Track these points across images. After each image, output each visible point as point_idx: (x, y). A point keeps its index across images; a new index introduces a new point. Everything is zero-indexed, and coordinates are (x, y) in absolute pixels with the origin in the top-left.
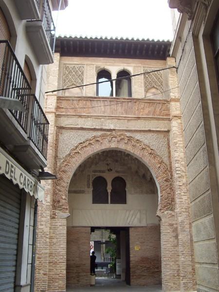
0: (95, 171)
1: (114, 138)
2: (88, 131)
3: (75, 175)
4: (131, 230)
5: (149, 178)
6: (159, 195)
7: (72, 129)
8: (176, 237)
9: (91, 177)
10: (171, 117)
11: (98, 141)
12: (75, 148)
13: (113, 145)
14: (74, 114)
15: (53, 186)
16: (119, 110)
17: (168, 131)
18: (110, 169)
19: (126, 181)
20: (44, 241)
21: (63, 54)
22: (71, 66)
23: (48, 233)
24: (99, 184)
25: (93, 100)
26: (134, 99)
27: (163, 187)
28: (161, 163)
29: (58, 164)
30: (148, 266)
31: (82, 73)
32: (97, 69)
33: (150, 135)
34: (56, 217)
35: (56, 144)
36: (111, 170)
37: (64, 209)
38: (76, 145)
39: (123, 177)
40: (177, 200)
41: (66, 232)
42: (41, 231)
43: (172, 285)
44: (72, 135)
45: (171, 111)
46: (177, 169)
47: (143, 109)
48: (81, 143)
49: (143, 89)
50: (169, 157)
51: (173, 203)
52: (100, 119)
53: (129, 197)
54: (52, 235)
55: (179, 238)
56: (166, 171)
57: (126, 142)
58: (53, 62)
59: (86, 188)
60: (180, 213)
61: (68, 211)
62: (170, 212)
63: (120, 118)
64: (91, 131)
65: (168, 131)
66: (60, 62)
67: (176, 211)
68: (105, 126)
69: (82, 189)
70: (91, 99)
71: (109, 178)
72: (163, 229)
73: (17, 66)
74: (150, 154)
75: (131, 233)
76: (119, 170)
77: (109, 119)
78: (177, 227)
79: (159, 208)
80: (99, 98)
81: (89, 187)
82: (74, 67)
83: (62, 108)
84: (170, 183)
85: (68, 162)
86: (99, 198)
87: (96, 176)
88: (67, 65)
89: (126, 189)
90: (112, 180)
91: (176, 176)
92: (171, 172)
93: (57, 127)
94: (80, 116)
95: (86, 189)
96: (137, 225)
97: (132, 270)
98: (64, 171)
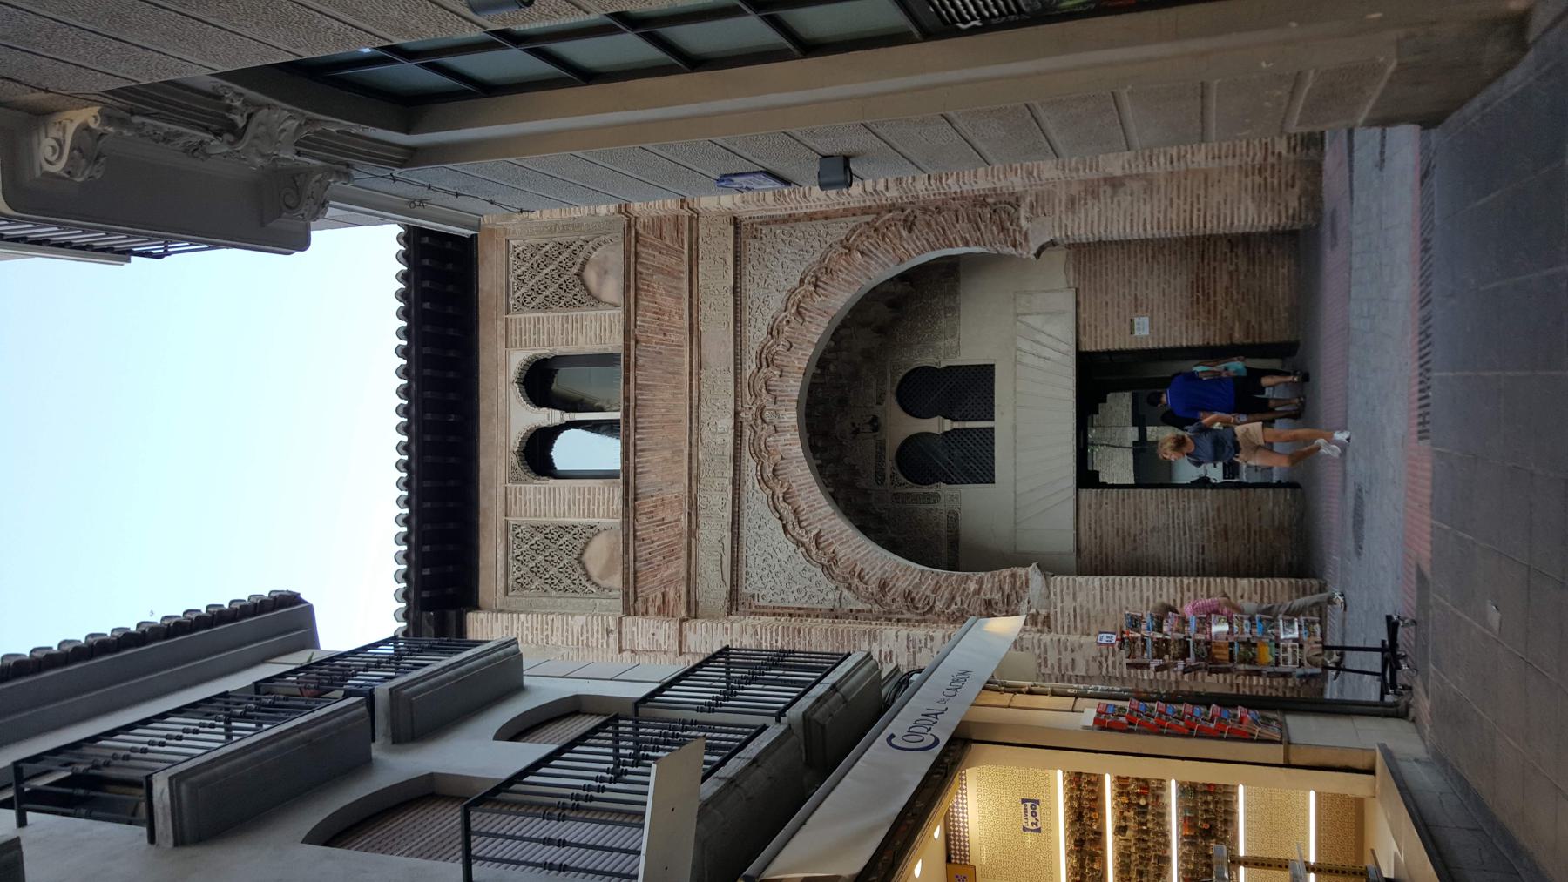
0: (880, 475)
1: (767, 415)
2: (744, 507)
3: (893, 547)
4: (1089, 346)
5: (900, 286)
6: (961, 250)
7: (735, 562)
8: (1115, 183)
9: (899, 490)
10: (685, 213)
11: (774, 470)
13: (790, 417)
14: (684, 554)
16: (664, 402)
17: (736, 222)
18: (871, 422)
21: (471, 602)
22: (512, 569)
26: (627, 347)
29: (860, 606)
30: (1225, 278)
32: (524, 477)
33: (748, 288)
37: (1013, 587)
38: (793, 547)
41: (1097, 579)
43: (1297, 189)
47: (659, 313)
48: (784, 527)
49: (589, 313)
50: (826, 218)
51: (990, 200)
53: (970, 355)
55: (1118, 173)
57: (777, 372)
58: (514, 642)
59: (940, 506)
60: (1031, 173)
61: (1021, 571)
62: (1023, 212)
63: (695, 394)
64: (744, 496)
65: (736, 222)
66: (501, 611)
67: (1019, 189)
68: (723, 445)
70: (631, 496)
72: (1082, 235)
73: (543, 770)
74: (816, 286)
75: (1102, 347)
77: (699, 435)
78: (1080, 181)
79: (1011, 250)
80: (625, 468)
81: (936, 497)
84: (918, 213)
86: (975, 460)
87: (897, 471)
89: (943, 365)
90: (904, 416)
91: (893, 193)
92: (878, 211)
93: (730, 613)
94: (692, 533)
97: (1238, 337)
98: (883, 586)
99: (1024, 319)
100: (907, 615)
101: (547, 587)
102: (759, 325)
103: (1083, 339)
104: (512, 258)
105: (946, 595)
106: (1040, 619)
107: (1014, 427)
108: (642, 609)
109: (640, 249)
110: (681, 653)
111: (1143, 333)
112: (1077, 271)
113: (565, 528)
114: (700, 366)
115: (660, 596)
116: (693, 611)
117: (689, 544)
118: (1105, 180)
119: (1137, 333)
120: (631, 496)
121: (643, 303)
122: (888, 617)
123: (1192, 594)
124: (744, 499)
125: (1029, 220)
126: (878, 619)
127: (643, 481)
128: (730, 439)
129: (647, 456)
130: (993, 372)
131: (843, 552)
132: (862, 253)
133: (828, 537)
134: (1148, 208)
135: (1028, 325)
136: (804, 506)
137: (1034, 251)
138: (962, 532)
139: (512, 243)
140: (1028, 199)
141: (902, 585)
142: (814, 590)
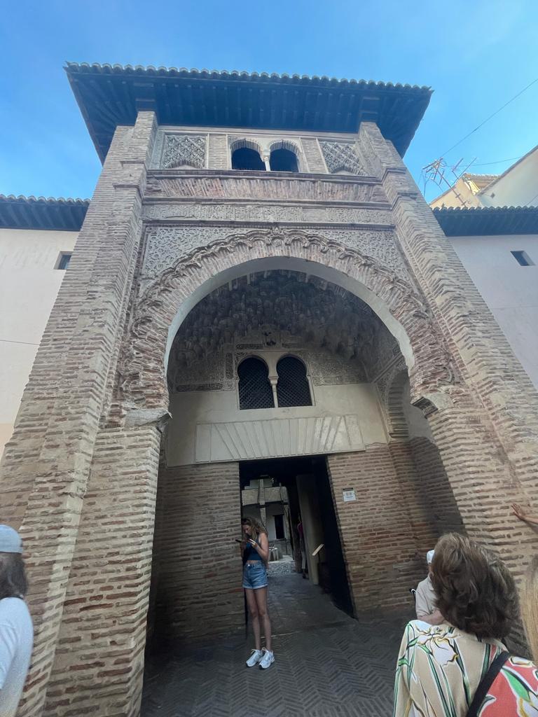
2: (218, 229)
6: (407, 350)
8: (501, 455)
9: (234, 357)
11: (241, 244)
12: (187, 257)
13: (277, 252)
15: (123, 339)
19: (306, 363)
20: (51, 510)
23: (73, 475)
25: (227, 179)
26: (310, 176)
27: (414, 329)
28: (392, 282)
29: (142, 290)
31: (203, 146)
32: (232, 141)
34: (123, 421)
35: (140, 253)
38: (188, 252)
39: (298, 355)
40: (464, 355)
42: (47, 468)
45: (388, 195)
46: (441, 283)
48: (203, 248)
52: (245, 205)
54: (95, 483)
56: (409, 296)
57: (306, 245)
59: (225, 379)
63: (287, 204)
67: (468, 382)
70: (221, 176)
74: (365, 265)
77: (262, 206)
78: (493, 427)
82: (186, 139)
83: (160, 191)
88: (172, 136)
89: (309, 378)
91: (439, 301)
93: (144, 222)
94: (198, 201)
96: (344, 450)
98: (156, 304)
100: (131, 320)
101: (169, 149)
102: (335, 236)
103: (335, 458)
104: (346, 144)
105: (145, 346)
106: (116, 419)
107: (276, 419)
108: (151, 181)
109: (366, 186)
110: (116, 186)
111: (345, 498)
112: (376, 451)
113: (203, 156)
115: (159, 189)
116: (147, 203)
117: (191, 200)
118: (501, 446)
119: (344, 493)
120: (221, 176)
121: (336, 186)
122: (131, 308)
123: (123, 574)
124: (221, 228)
125: (447, 392)
126: (131, 301)
127: (232, 182)
128: (261, 220)
129: (246, 183)
130: (308, 405)
131: (184, 281)
132: (392, 289)
133: (194, 271)
134: (494, 487)
135: (339, 423)
137: (425, 396)
139: (354, 146)
140: (463, 390)
141: (157, 316)
142: (156, 264)
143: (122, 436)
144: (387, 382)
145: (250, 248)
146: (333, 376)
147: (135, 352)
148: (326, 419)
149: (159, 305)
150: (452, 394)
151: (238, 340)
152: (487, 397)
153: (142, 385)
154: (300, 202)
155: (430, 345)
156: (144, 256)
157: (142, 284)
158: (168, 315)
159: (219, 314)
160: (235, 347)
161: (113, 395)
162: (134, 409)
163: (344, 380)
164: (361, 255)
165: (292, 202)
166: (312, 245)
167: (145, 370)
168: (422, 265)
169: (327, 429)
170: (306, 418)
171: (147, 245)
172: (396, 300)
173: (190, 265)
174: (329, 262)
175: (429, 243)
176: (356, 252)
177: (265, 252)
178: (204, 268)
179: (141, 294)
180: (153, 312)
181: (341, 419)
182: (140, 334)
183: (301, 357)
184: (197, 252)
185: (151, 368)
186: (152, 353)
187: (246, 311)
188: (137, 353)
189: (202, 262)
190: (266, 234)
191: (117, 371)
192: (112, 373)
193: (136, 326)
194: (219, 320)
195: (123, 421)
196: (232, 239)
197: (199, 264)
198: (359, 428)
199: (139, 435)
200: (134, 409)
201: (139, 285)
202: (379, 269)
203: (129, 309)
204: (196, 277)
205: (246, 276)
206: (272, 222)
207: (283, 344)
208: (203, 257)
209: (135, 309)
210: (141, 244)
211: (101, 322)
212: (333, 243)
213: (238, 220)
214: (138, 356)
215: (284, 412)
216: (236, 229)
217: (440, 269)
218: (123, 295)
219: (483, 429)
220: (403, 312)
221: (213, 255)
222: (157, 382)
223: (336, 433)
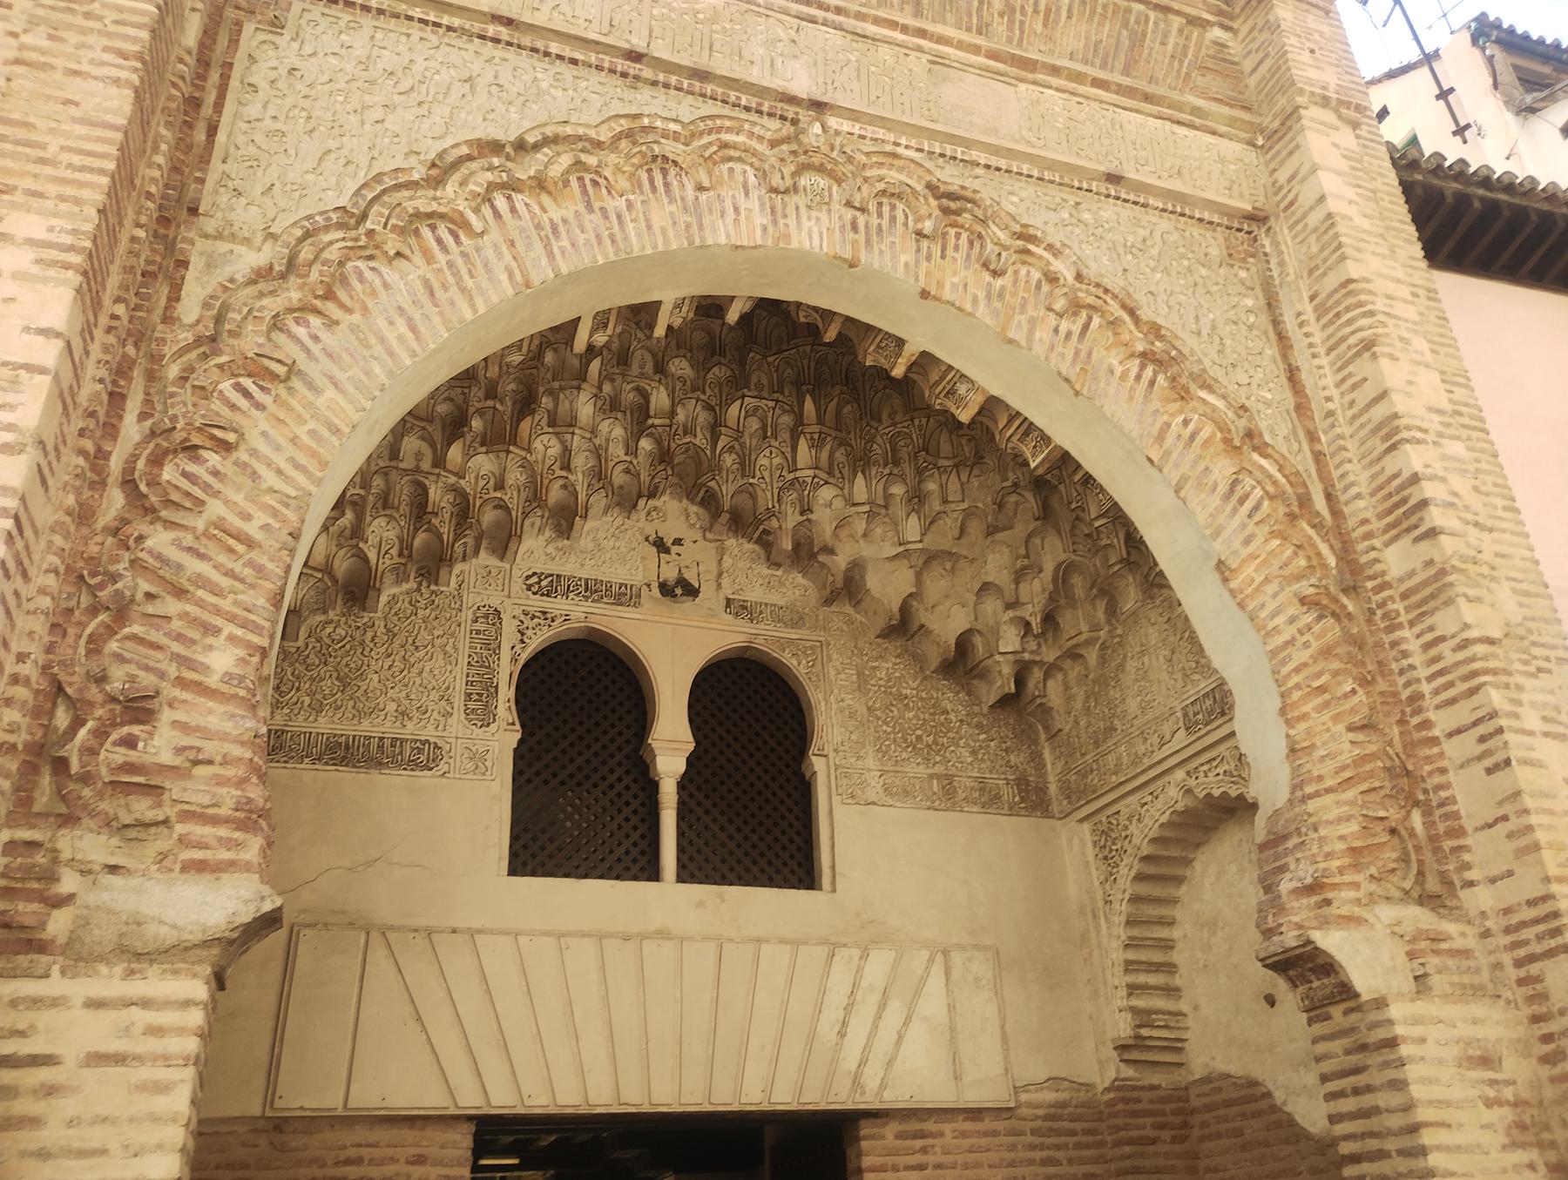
13: (815, 231)
15: (84, 515)
18: (682, 582)
24: (576, 701)
34: (59, 924)
36: (692, 591)
39: (787, 658)
44: (387, 60)
45: (1252, 81)
48: (496, 147)
59: (457, 725)
63: (871, 29)
69: (410, 730)
71: (672, 655)
76: (755, 594)
85: (329, 295)
89: (818, 764)
95: (457, 730)
98: (259, 370)
99: (938, 968)
105: (194, 565)
114: (937, 61)
128: (756, 75)
136: (555, 213)
138: (378, 778)
141: (258, 430)
143: (56, 1002)
144: (1133, 828)
145: (700, 188)
146: (917, 769)
147: (144, 586)
148: (873, 953)
149: (274, 377)
150: (1414, 940)
151: (537, 550)
152: (1534, 969)
153: (167, 758)
154: (922, 33)
155: (1351, 729)
156: (212, 130)
157: (197, 263)
158: (312, 433)
159: (477, 424)
160: (518, 586)
161: (17, 789)
162: (113, 869)
163: (961, 795)
164: (1132, 312)
165: (893, 25)
166: (952, 231)
167: (180, 682)
168: (1352, 404)
169: (873, 1000)
170: (796, 943)
171: (236, 74)
172: (1243, 526)
173: (430, 215)
174: (1009, 318)
175: (1391, 322)
176: (1115, 297)
177: (760, 219)
178: (495, 234)
179: (190, 308)
180: (243, 403)
181: (931, 960)
182: (168, 503)
183: (797, 666)
184: (470, 158)
185: (213, 681)
186: (226, 604)
187: (594, 432)
188: (150, 596)
189: (486, 211)
190: (774, 144)
191: (46, 668)
192: (27, 682)
193: (157, 461)
194: (468, 456)
195: (59, 924)
196: (629, 134)
197: (472, 218)
198: (1001, 1009)
199: (145, 1003)
200: (113, 869)
201: (184, 264)
202: (1193, 387)
203: (122, 370)
204: (456, 274)
205: (655, 306)
206: (805, 96)
207: (729, 602)
208: (491, 187)
209: (151, 377)
210: (204, 63)
211: (10, 427)
212: (1032, 239)
213: (660, 51)
214: (150, 609)
215: (700, 904)
216: (645, 93)
217: (1419, 435)
218: (107, 301)
219: (1508, 1094)
220: (1267, 580)
221: (540, 184)
222: (237, 751)
223: (908, 1021)
